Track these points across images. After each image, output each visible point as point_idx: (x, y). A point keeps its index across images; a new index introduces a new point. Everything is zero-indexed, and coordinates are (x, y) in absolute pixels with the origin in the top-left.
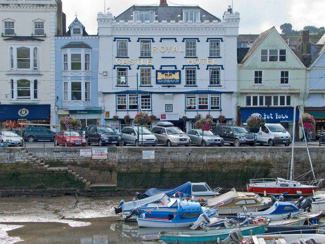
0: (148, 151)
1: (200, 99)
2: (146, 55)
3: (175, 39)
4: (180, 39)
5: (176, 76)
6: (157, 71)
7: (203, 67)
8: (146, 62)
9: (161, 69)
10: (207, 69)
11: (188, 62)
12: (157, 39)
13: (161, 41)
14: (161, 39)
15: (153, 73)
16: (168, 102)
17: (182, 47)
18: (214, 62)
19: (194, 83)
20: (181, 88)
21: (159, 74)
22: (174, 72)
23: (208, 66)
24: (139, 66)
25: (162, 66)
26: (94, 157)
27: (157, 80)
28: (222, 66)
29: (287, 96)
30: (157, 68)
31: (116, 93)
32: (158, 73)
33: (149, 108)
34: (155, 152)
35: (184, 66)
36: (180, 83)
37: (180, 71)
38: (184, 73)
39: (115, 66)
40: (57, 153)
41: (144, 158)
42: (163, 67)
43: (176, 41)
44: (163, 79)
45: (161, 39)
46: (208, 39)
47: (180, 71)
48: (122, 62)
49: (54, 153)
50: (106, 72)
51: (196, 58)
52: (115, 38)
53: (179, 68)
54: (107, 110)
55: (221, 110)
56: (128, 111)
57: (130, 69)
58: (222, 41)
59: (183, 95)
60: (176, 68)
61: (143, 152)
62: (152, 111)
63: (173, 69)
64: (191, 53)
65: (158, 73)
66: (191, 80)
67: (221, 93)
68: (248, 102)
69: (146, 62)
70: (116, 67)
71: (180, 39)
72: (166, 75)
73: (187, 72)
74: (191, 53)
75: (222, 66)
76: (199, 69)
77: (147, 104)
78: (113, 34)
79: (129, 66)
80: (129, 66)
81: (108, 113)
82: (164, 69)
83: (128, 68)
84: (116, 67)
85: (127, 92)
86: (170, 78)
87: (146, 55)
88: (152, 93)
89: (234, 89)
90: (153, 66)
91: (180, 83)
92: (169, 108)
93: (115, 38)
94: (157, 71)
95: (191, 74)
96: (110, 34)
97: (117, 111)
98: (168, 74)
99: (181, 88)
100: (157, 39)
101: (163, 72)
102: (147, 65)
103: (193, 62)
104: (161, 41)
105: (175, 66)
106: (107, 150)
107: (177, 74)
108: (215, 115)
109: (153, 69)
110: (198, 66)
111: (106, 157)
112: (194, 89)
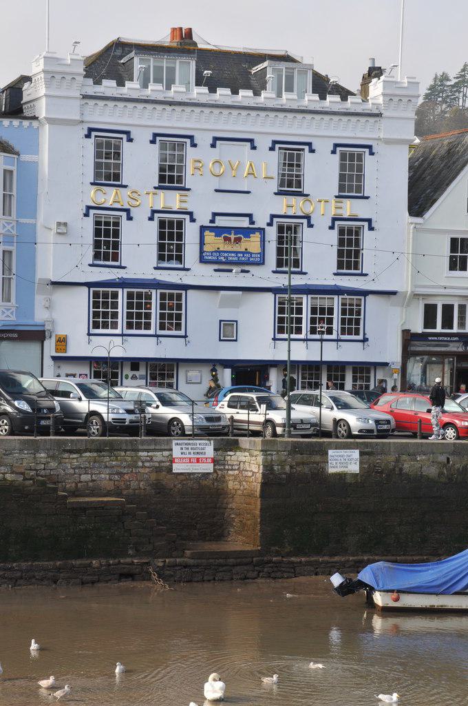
0: (342, 452)
1: (314, 311)
2: (170, 178)
3: (251, 141)
4: (263, 143)
5: (253, 244)
6: (203, 229)
8: (172, 200)
9: (212, 221)
10: (332, 228)
11: (283, 205)
12: (204, 140)
13: (213, 146)
14: (216, 139)
15: (191, 233)
16: (227, 314)
17: (270, 163)
18: (350, 208)
19: (116, 257)
21: (210, 237)
22: (247, 232)
23: (334, 220)
24: (154, 212)
25: (215, 214)
26: (178, 468)
27: (201, 251)
28: (369, 221)
29: (444, 306)
31: (89, 285)
32: (207, 233)
33: (178, 327)
34: (361, 454)
35: (273, 216)
36: (261, 262)
37: (262, 231)
38: (272, 233)
39: (89, 208)
40: (75, 456)
41: (331, 470)
43: (254, 148)
44: (218, 251)
45: (216, 139)
46: (275, 142)
48: (109, 197)
49: (66, 455)
50: (65, 224)
51: (300, 194)
52: (91, 130)
53: (261, 221)
54: (61, 331)
55: (365, 340)
56: (122, 335)
57: (130, 218)
58: (372, 153)
59: (270, 296)
60: (252, 222)
61: (331, 452)
62: (185, 337)
63: (245, 223)
64: (291, 185)
65: (207, 233)
66: (288, 258)
67: (366, 293)
68: (429, 320)
69: (172, 200)
70: (92, 212)
71: (263, 143)
72: (226, 239)
73: (281, 229)
74: (291, 185)
75: (369, 221)
76: (310, 226)
77: (173, 319)
78: (86, 119)
79: (128, 211)
80: (128, 211)
81: (62, 342)
82: (221, 222)
83: (124, 214)
84: (92, 212)
85: (123, 284)
86: (237, 248)
87: (170, 178)
89: (402, 282)
90: (191, 214)
91: (261, 262)
92: (228, 330)
93: (91, 130)
94: (203, 229)
95: (288, 235)
96: (78, 118)
97: (89, 334)
98: (233, 237)
99: (266, 275)
100: (204, 140)
101: (219, 231)
102: (175, 209)
103: (295, 206)
104: (213, 146)
105: (250, 216)
106: (212, 447)
107: (256, 238)
108: (349, 352)
110: (308, 217)
111: (209, 468)
112: (297, 281)
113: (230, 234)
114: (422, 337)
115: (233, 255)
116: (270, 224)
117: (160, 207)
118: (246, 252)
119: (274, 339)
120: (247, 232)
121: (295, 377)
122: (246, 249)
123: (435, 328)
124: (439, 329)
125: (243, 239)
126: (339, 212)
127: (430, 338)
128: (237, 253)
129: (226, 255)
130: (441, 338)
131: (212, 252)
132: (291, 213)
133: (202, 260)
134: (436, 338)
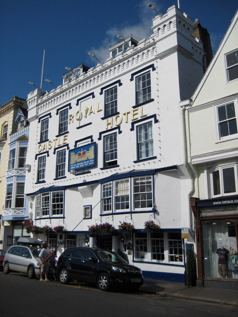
2: (63, 130)
3: (92, 94)
5: (90, 154)
6: (70, 151)
7: (126, 127)
9: (75, 146)
13: (77, 104)
17: (99, 101)
20: (97, 174)
25: (76, 142)
30: (72, 147)
36: (95, 166)
38: (100, 144)
42: (78, 143)
47: (95, 145)
60: (92, 140)
62: (64, 218)
63: (89, 141)
71: (97, 92)
72: (80, 154)
75: (154, 116)
86: (84, 159)
88: (65, 188)
99: (97, 174)
105: (91, 137)
109: (68, 148)
113: (81, 151)
114: (208, 204)
115: (82, 163)
116: (100, 139)
117: (57, 147)
118: (88, 160)
119: (101, 215)
120: (87, 147)
121: (131, 242)
122: (87, 158)
123: (220, 193)
124: (222, 194)
125: (86, 152)
126: (136, 117)
127: (214, 203)
128: (83, 161)
129: (79, 164)
130: (224, 202)
131: (73, 164)
132: (109, 128)
133: (69, 171)
134: (220, 203)
